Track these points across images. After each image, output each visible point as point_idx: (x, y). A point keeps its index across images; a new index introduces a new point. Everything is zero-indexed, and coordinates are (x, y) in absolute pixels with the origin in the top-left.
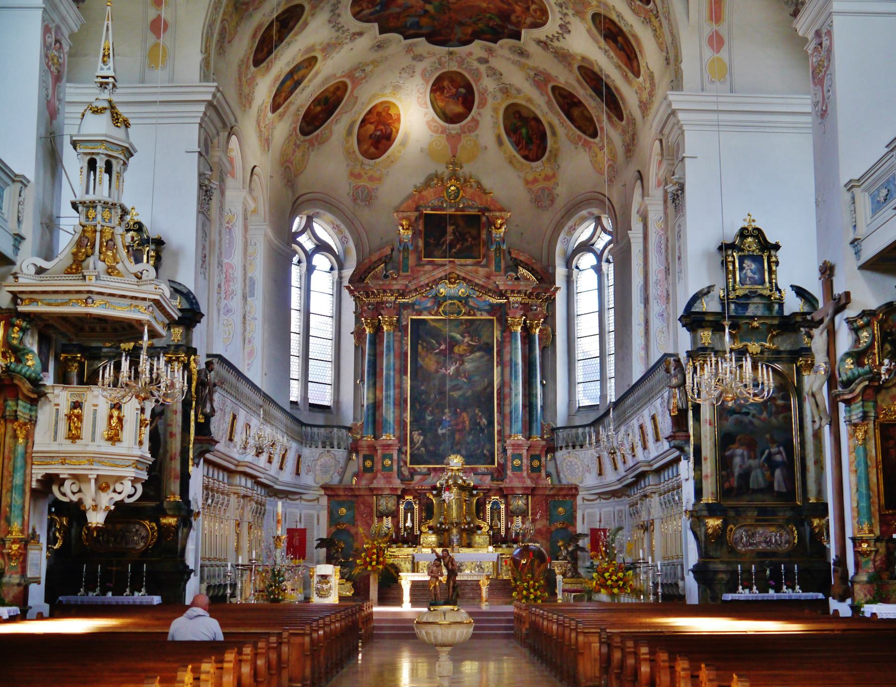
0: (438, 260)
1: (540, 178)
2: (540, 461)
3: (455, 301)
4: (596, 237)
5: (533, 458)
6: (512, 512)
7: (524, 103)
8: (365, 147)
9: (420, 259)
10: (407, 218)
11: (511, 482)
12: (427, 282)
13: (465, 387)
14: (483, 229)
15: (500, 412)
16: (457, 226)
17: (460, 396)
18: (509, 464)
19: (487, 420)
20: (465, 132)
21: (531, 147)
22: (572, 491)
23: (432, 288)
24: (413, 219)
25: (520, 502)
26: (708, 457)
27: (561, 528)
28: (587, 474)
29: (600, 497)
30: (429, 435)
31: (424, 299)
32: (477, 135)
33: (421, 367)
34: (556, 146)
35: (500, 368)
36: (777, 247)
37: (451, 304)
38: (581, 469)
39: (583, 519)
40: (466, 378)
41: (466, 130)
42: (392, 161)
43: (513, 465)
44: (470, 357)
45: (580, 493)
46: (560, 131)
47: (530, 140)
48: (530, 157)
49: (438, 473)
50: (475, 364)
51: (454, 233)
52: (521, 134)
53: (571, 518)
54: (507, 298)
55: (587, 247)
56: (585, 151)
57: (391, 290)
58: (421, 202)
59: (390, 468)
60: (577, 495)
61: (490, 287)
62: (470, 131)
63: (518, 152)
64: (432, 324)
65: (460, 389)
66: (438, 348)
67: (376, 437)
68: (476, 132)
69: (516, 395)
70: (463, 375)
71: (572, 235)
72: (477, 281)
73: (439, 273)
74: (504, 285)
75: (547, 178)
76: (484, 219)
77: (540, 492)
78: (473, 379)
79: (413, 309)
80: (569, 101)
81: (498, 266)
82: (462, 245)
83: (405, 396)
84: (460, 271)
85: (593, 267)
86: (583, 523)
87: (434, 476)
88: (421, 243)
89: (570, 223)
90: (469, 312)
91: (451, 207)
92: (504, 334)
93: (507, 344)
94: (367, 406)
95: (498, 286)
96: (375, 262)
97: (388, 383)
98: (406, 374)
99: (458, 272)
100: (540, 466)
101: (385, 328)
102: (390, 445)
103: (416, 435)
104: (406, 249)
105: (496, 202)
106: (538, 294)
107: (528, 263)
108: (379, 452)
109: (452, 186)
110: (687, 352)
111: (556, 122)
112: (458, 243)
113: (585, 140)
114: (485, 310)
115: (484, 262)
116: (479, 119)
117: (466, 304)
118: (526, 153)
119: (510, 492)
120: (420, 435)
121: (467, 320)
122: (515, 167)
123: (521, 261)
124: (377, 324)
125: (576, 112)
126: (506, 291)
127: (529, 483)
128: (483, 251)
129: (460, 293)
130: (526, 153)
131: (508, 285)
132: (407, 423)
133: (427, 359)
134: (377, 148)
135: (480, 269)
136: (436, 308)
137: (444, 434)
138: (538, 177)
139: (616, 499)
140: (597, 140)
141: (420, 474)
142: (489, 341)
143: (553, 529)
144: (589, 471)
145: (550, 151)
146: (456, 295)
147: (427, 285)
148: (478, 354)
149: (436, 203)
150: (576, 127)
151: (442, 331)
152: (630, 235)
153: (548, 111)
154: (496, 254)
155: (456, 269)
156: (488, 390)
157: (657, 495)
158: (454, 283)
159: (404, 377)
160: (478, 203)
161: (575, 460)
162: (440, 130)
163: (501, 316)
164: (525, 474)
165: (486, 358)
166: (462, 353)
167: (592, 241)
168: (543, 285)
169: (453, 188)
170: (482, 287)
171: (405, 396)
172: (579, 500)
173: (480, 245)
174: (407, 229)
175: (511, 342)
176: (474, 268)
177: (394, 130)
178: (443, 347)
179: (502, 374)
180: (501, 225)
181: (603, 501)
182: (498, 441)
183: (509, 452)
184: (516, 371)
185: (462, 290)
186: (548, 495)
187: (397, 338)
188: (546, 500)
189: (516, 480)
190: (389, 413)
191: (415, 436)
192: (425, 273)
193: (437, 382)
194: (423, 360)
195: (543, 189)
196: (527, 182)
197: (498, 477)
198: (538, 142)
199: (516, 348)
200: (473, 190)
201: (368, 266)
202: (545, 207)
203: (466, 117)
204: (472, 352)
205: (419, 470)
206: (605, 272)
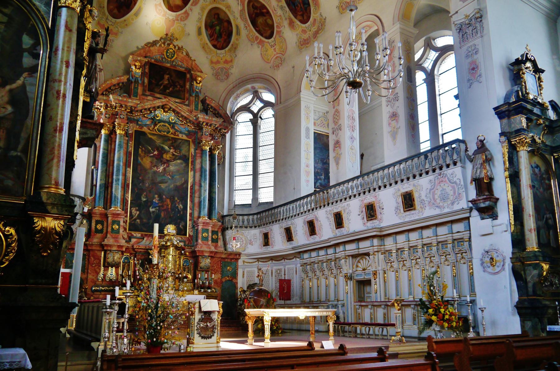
0: (158, 96)
1: (222, 61)
2: (218, 235)
3: (167, 125)
4: (253, 103)
5: (213, 232)
6: (201, 268)
7: (224, 9)
8: (111, 7)
9: (145, 91)
10: (140, 61)
11: (201, 247)
12: (149, 107)
13: (169, 181)
14: (188, 82)
15: (192, 201)
16: (171, 76)
17: (166, 187)
18: (200, 236)
19: (183, 205)
20: (177, 20)
21: (220, 40)
22: (236, 256)
23: (151, 112)
24: (143, 63)
25: (207, 261)
26: (531, 214)
27: (229, 280)
28: (249, 246)
29: (258, 261)
30: (143, 212)
31: (144, 119)
32: (185, 24)
33: (140, 164)
34: (237, 42)
35: (192, 172)
36: (543, 71)
37: (163, 125)
38: (244, 242)
39: (244, 274)
40: (170, 176)
41: (179, 19)
42: (126, 25)
43: (202, 236)
44: (174, 162)
45: (241, 258)
46: (244, 32)
47: (220, 35)
48: (218, 46)
49: (150, 238)
50: (176, 167)
51: (168, 79)
52: (216, 29)
53: (235, 275)
54: (201, 129)
55: (246, 108)
56: (259, 47)
57: (126, 106)
58: (149, 54)
59: (118, 231)
60: (240, 258)
61: (191, 119)
62: (181, 20)
63: (210, 41)
64: (150, 136)
65: (166, 183)
66: (153, 153)
67: (105, 207)
68: (185, 22)
69: (205, 191)
70: (168, 174)
71: (237, 100)
72: (183, 113)
73: (158, 103)
74: (203, 118)
75: (226, 62)
76: (188, 76)
77: (218, 256)
78: (175, 177)
79: (137, 124)
80: (259, 12)
81: (197, 107)
82: (173, 89)
83: (128, 182)
84: (172, 104)
85: (251, 120)
86: (243, 277)
87: (146, 240)
88: (146, 81)
89: (239, 92)
90: (175, 133)
91: (168, 63)
92: (197, 151)
93: (198, 158)
94: (100, 186)
95: (198, 118)
96: (114, 85)
97: (118, 170)
98: (129, 166)
99: (170, 105)
100: (217, 239)
101: (118, 132)
102: (119, 214)
103: (134, 211)
104: (136, 82)
105: (198, 66)
106: (220, 130)
107: (216, 108)
108: (110, 219)
109: (171, 49)
110: (500, 134)
111: (242, 25)
112: (170, 87)
113: (260, 39)
114: (185, 134)
115: (187, 103)
116: (190, 13)
117: (173, 127)
118: (216, 43)
119: (201, 254)
120: (136, 210)
121: (172, 138)
122: (205, 51)
123: (212, 107)
124: (111, 128)
125: (260, 20)
126: (203, 122)
127: (213, 249)
128: (187, 95)
129: (170, 119)
130: (216, 43)
131: (205, 119)
132: (128, 201)
133: (144, 159)
134: (119, 11)
135: (184, 107)
136: (152, 126)
137: (153, 212)
138: (220, 60)
139: (274, 262)
140: (270, 41)
141: (136, 238)
142: (187, 154)
143: (224, 280)
144: (251, 243)
145: (232, 45)
146: (167, 120)
147: (149, 109)
148: (179, 161)
149: (158, 57)
150: (256, 30)
151: (156, 142)
152: (301, 96)
153: (239, 18)
154: (195, 99)
155: (170, 103)
156: (184, 186)
157: (380, 253)
158: (167, 112)
159: (128, 169)
160: (185, 65)
161: (241, 236)
162: (163, 13)
163: (195, 139)
164: (210, 243)
165: (184, 165)
166: (168, 159)
167: (250, 106)
168: (225, 124)
169: (171, 50)
170: (186, 118)
171: (128, 182)
172: (240, 262)
173: (185, 92)
174: (138, 69)
175: (201, 157)
176: (180, 105)
177: (133, 2)
178: (156, 153)
179: (194, 177)
180: (200, 82)
181: (260, 263)
182: (190, 220)
183: (200, 228)
184: (205, 175)
185: (171, 117)
186: (222, 258)
187: (126, 142)
188: (221, 261)
189: (204, 246)
190: (117, 191)
191: (133, 211)
192: (148, 100)
193: (150, 175)
194: (142, 159)
195: (222, 69)
196: (212, 62)
197: (188, 243)
198: (225, 37)
199: (206, 161)
200: (182, 56)
201: (109, 86)
202: (222, 80)
203: (182, 9)
204: (174, 160)
205: (135, 235)
206: (259, 125)
